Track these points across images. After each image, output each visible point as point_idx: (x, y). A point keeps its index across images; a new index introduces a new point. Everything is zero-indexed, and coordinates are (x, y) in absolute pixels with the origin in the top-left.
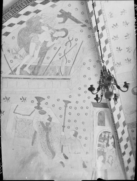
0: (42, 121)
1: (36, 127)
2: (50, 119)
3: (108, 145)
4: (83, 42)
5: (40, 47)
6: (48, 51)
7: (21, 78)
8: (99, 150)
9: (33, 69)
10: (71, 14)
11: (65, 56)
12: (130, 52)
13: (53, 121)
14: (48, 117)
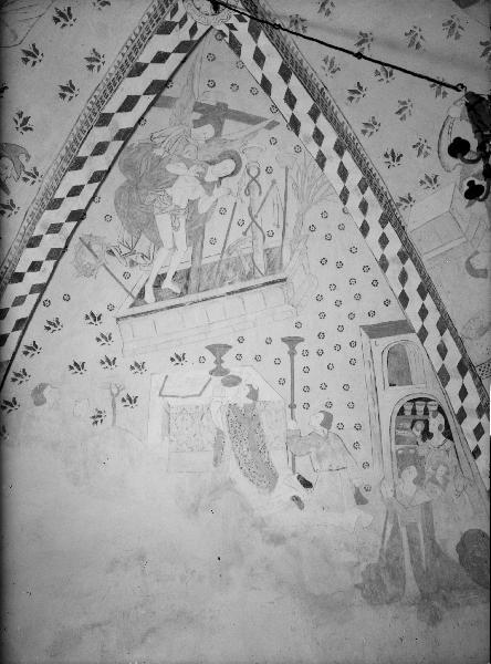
0: (232, 402)
1: (219, 420)
2: (254, 394)
3: (427, 434)
5: (182, 220)
6: (208, 225)
7: (162, 310)
8: (400, 452)
9: (185, 279)
10: (225, 105)
12: (426, 154)
13: (261, 398)
14: (248, 390)
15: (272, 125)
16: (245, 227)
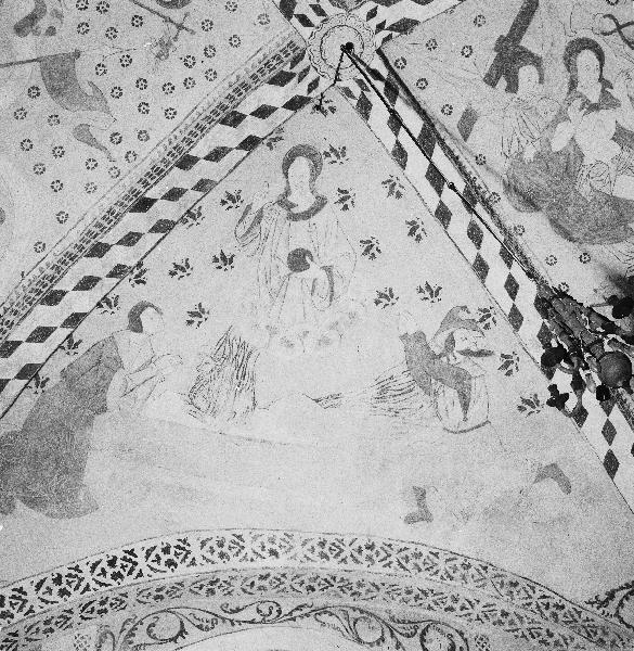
10: (501, 40)
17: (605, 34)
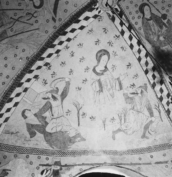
4: (38, 29)
11: (16, 21)
12: (52, 77)
15: (54, 20)
16: (14, 17)
17: (35, 12)
